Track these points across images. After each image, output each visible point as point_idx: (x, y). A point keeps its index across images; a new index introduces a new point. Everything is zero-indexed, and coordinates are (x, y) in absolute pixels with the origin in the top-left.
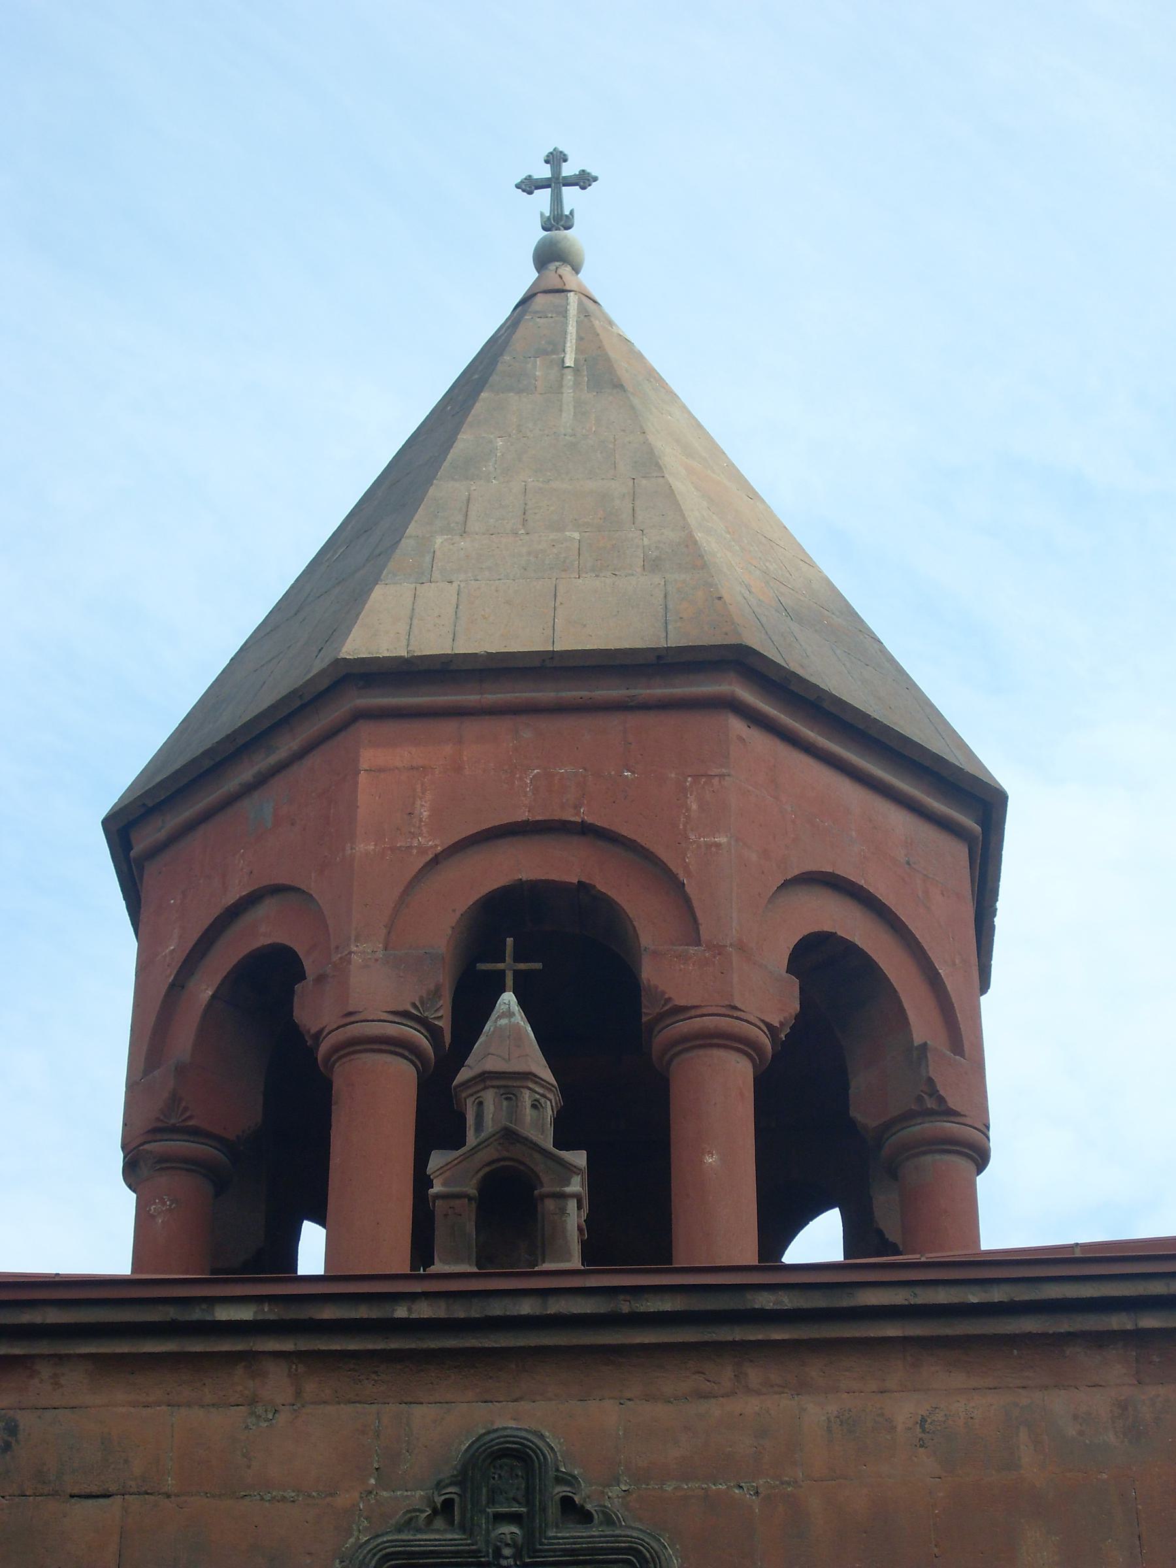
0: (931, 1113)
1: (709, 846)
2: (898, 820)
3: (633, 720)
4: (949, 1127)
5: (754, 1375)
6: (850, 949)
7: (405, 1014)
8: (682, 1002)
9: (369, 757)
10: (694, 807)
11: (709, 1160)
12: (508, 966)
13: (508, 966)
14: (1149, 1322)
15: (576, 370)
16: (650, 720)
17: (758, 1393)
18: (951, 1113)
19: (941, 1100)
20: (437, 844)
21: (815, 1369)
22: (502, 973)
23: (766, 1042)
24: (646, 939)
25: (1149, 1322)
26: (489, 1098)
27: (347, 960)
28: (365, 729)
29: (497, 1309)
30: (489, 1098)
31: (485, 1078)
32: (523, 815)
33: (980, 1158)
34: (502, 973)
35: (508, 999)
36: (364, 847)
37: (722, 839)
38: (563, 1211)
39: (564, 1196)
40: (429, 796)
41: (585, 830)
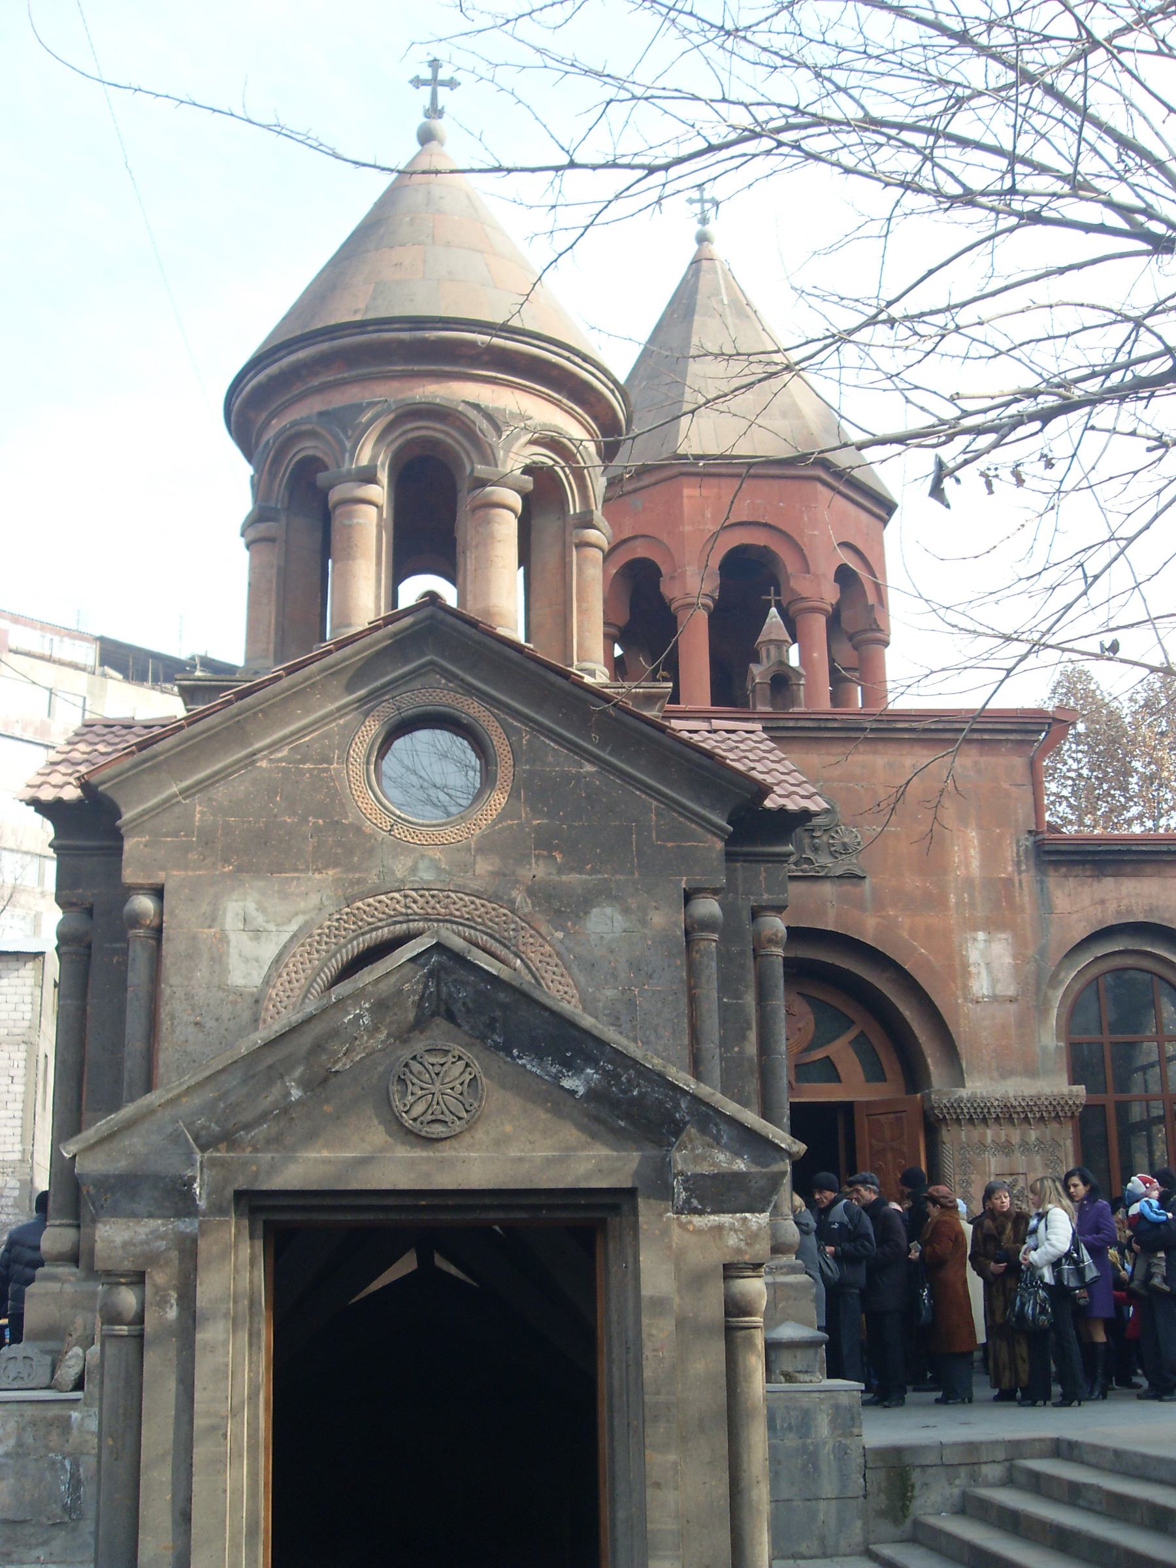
0: (873, 630)
1: (812, 535)
2: (864, 516)
3: (783, 482)
4: (879, 635)
5: (861, 748)
6: (854, 574)
7: (707, 595)
8: (805, 596)
9: (686, 492)
10: (806, 519)
11: (815, 655)
12: (772, 598)
13: (772, 598)
14: (986, 737)
15: (729, 306)
16: (789, 483)
17: (862, 754)
18: (880, 630)
19: (878, 626)
20: (715, 528)
21: (880, 747)
22: (770, 600)
23: (830, 609)
24: (790, 570)
25: (986, 737)
26: (772, 648)
27: (684, 572)
28: (685, 480)
29: (781, 724)
30: (772, 648)
31: (771, 641)
32: (744, 519)
33: (886, 644)
34: (770, 600)
35: (773, 610)
36: (688, 528)
37: (816, 533)
38: (799, 690)
39: (800, 685)
40: (710, 509)
41: (766, 525)
